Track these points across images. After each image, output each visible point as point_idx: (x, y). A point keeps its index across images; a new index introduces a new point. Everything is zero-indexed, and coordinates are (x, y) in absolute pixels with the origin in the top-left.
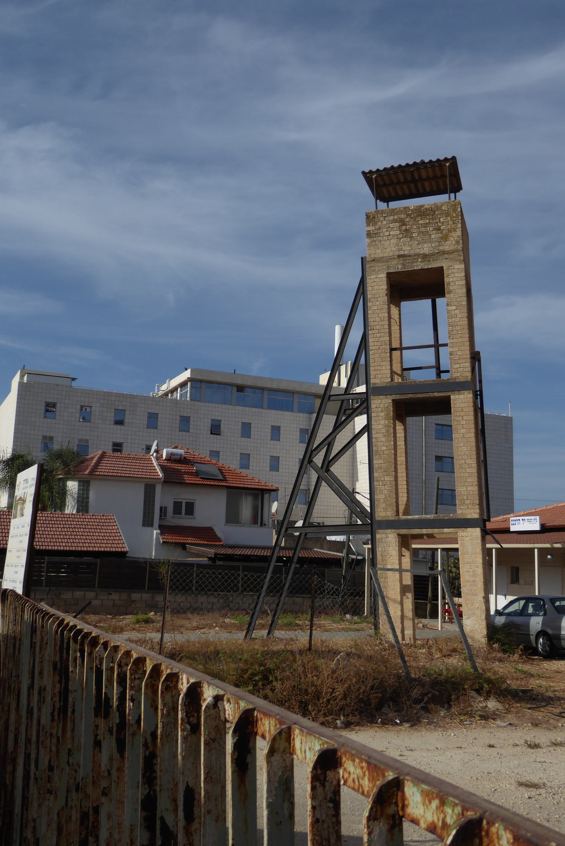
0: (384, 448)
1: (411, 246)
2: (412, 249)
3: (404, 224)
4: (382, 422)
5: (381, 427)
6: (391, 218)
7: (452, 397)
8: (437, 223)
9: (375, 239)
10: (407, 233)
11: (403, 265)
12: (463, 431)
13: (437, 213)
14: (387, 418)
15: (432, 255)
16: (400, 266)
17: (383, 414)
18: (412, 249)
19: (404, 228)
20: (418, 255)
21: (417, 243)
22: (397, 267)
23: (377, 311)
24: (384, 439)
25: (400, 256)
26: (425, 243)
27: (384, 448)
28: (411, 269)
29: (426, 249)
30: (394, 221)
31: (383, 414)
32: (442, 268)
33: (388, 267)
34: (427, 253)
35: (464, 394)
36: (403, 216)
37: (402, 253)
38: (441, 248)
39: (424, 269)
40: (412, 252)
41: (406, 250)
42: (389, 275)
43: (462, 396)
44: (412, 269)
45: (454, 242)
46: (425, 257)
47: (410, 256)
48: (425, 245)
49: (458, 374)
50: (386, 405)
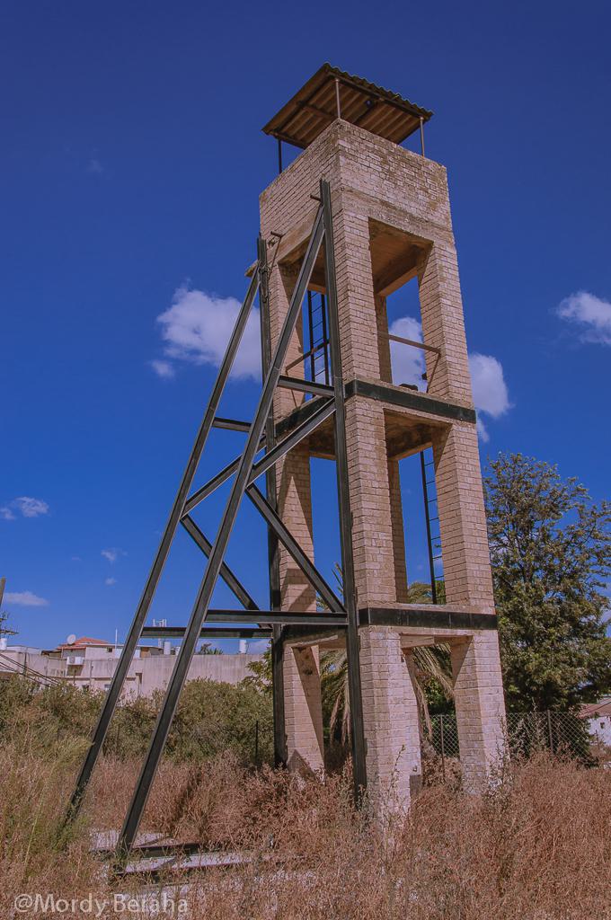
0: (376, 485)
2: (397, 201)
3: (386, 162)
5: (370, 448)
6: (371, 145)
7: (454, 427)
8: (424, 182)
9: (352, 162)
10: (390, 175)
11: (388, 216)
12: (470, 480)
13: (423, 168)
14: (377, 437)
15: (420, 220)
16: (384, 217)
17: (372, 428)
18: (397, 201)
19: (387, 167)
21: (403, 195)
23: (358, 266)
24: (374, 469)
25: (384, 203)
26: (411, 200)
27: (376, 485)
28: (397, 227)
30: (373, 151)
31: (372, 428)
32: (430, 245)
33: (370, 210)
34: (416, 215)
35: (467, 426)
36: (385, 152)
37: (385, 199)
38: (430, 217)
39: (412, 234)
40: (397, 205)
41: (391, 198)
43: (465, 429)
44: (399, 227)
45: (443, 217)
46: (412, 218)
47: (395, 208)
48: (413, 204)
49: (459, 397)
50: (376, 415)
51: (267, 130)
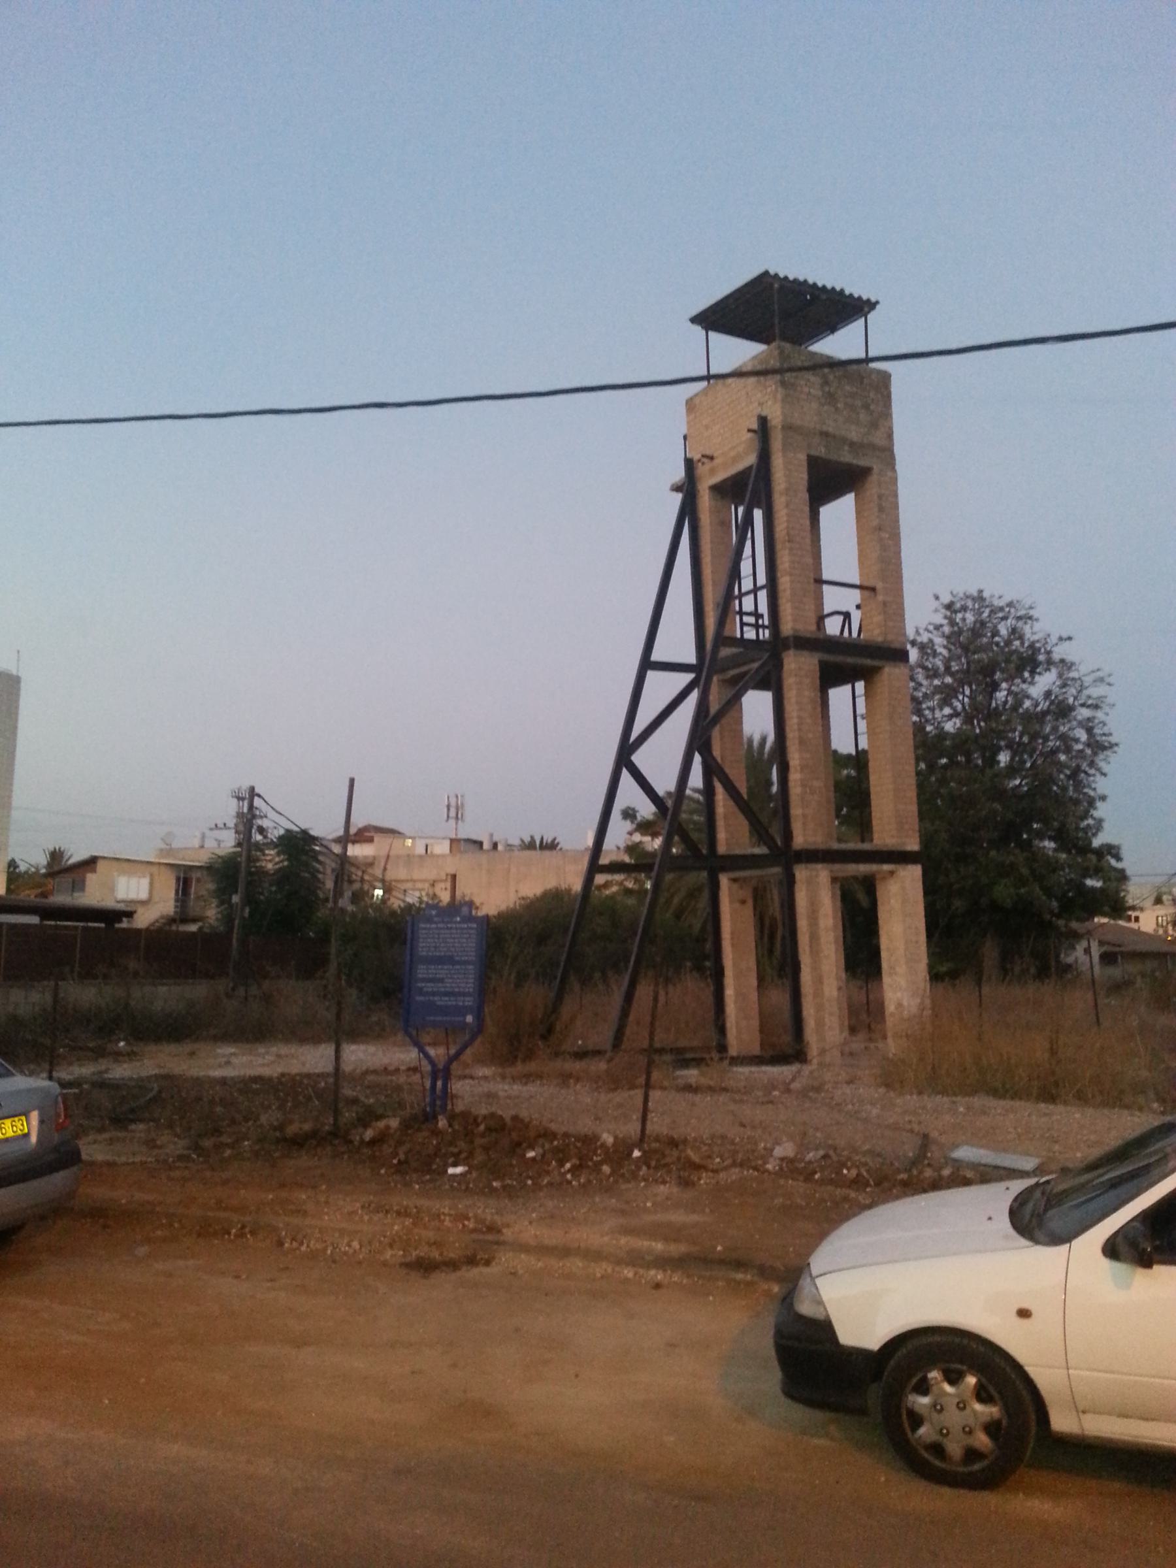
1: (836, 421)
4: (807, 693)
11: (826, 447)
15: (862, 446)
17: (807, 681)
19: (827, 389)
20: (844, 440)
22: (821, 451)
25: (825, 434)
29: (854, 434)
34: (855, 439)
37: (825, 428)
42: (808, 456)
43: (897, 671)
46: (852, 444)
47: (834, 437)
48: (853, 427)
51: (695, 320)
